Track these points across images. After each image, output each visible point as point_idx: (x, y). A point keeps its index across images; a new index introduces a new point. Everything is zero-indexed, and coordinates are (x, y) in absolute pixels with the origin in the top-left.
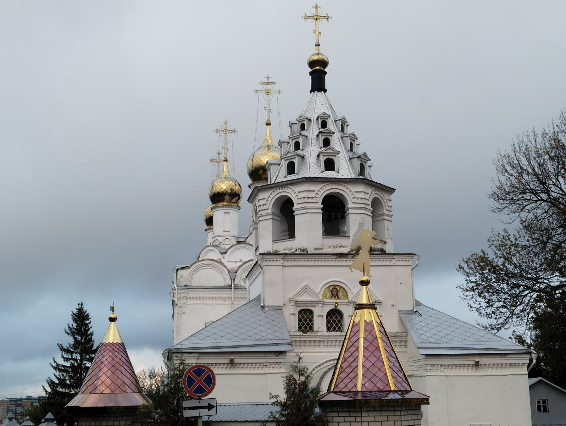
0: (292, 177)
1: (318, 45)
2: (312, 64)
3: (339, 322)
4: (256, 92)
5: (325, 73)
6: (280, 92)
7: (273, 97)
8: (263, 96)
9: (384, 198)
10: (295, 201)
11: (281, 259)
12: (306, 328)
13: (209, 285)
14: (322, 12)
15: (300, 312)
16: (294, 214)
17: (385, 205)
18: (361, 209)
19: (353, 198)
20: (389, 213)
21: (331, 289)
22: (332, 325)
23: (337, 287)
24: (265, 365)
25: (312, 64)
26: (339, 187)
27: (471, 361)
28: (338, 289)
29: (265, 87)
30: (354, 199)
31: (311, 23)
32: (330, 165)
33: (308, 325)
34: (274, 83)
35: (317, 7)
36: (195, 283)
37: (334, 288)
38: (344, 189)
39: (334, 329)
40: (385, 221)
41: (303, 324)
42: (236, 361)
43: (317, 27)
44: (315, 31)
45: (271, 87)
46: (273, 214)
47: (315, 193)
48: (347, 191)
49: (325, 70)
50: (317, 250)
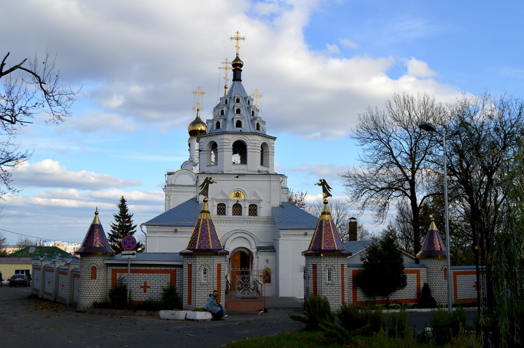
0: (218, 131)
3: (240, 210)
4: (220, 68)
5: (241, 71)
9: (269, 143)
10: (218, 144)
13: (185, 184)
14: (241, 35)
15: (218, 205)
20: (272, 151)
21: (236, 193)
22: (235, 212)
23: (239, 192)
26: (243, 137)
27: (303, 232)
28: (240, 193)
29: (225, 65)
31: (234, 42)
32: (239, 124)
33: (223, 212)
35: (238, 33)
36: (177, 183)
37: (237, 192)
38: (245, 138)
39: (237, 214)
41: (220, 211)
42: (178, 230)
43: (238, 44)
48: (247, 139)
49: (241, 69)
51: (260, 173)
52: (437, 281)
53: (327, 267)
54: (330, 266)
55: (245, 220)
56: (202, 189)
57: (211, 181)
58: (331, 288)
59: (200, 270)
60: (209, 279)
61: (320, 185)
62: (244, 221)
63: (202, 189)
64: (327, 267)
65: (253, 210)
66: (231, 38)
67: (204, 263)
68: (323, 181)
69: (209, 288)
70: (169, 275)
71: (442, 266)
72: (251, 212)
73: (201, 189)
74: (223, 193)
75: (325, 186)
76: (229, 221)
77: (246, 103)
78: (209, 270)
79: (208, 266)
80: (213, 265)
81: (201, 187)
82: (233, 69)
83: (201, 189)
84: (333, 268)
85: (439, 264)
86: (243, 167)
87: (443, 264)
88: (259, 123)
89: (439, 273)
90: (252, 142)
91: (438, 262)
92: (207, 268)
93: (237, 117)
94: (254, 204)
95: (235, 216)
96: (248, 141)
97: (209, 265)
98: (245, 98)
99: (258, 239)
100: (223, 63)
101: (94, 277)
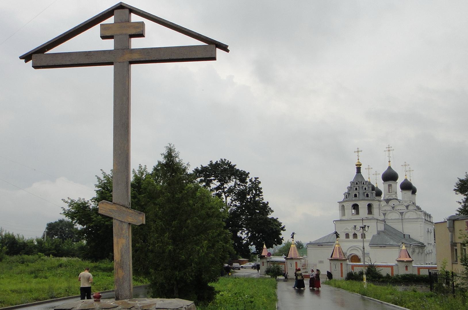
1: (358, 159)
4: (385, 151)
7: (391, 152)
8: (387, 153)
25: (357, 165)
31: (357, 153)
44: (357, 156)
45: (390, 149)
46: (341, 209)
66: (355, 152)
77: (361, 184)
82: (357, 167)
86: (358, 216)
98: (361, 182)
101: (263, 265)
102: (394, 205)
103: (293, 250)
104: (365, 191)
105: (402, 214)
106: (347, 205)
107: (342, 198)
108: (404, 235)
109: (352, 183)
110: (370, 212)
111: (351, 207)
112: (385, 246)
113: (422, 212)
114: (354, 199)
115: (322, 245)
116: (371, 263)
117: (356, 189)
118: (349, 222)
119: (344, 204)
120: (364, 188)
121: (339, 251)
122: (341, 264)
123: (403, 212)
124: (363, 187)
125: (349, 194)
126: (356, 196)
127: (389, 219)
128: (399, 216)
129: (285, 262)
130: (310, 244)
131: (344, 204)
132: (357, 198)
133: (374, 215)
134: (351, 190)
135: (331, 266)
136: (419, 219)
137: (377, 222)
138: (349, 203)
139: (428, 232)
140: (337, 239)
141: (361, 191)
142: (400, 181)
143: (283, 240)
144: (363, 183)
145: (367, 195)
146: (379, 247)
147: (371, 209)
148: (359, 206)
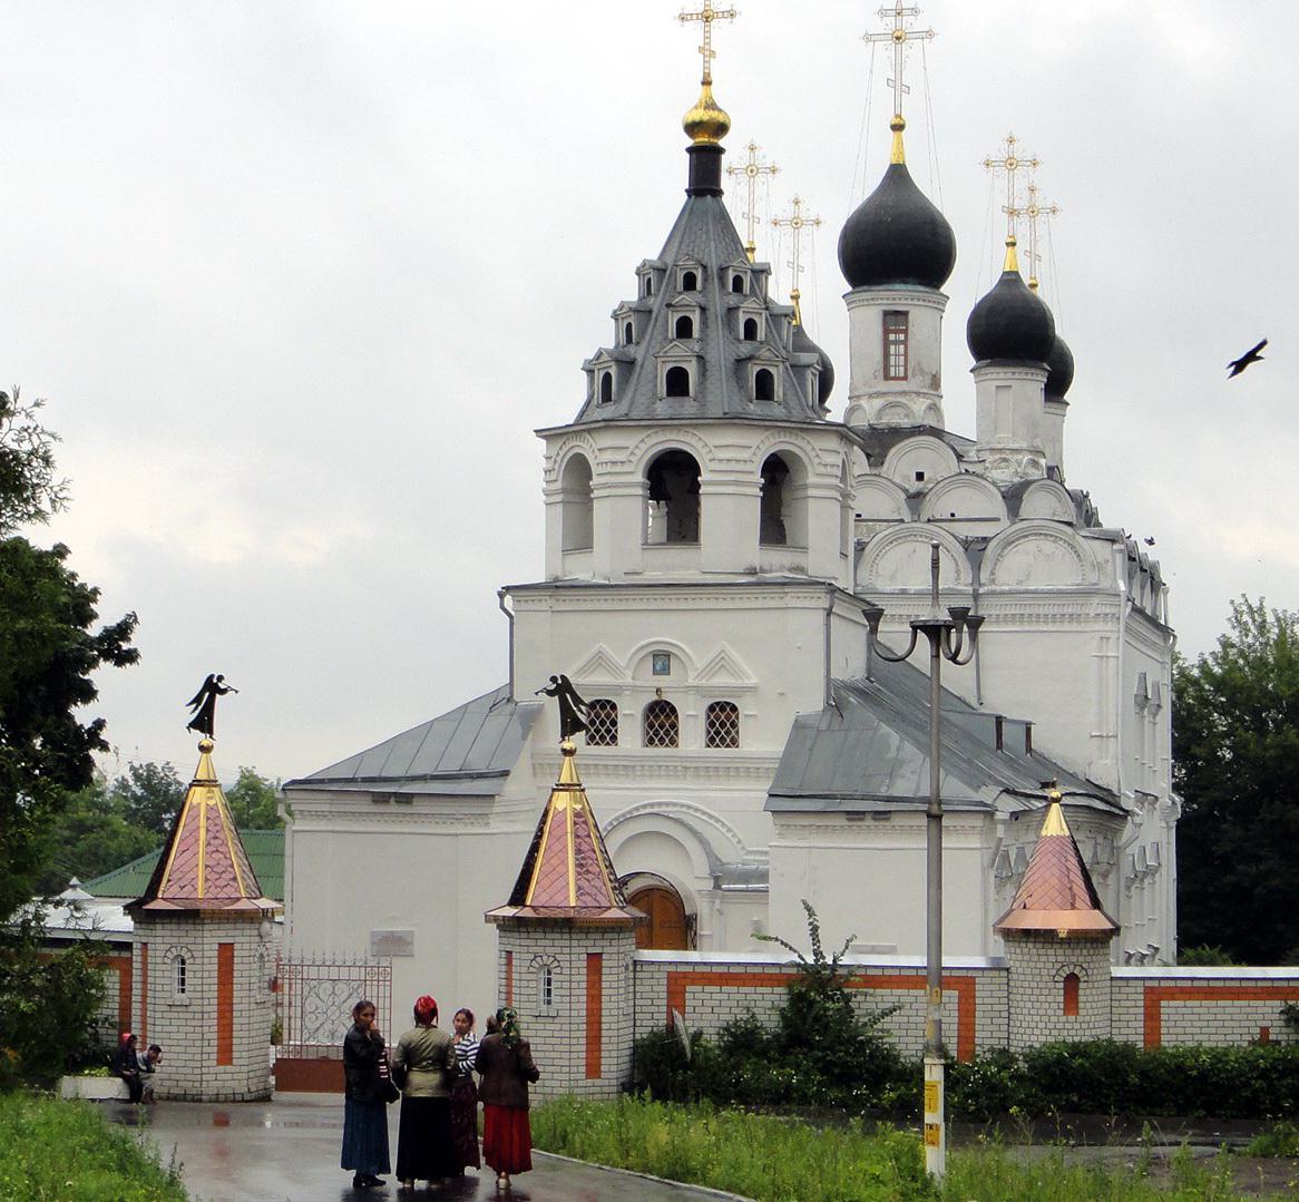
0: (609, 411)
1: (707, 83)
2: (692, 128)
4: (868, 38)
5: (720, 151)
6: (930, 34)
7: (912, 49)
8: (885, 51)
9: (808, 448)
11: (547, 598)
12: (602, 738)
16: (592, 496)
17: (812, 464)
18: (736, 483)
19: (710, 460)
24: (455, 818)
25: (692, 128)
30: (712, 463)
31: (696, 28)
33: (608, 731)
34: (915, 11)
38: (693, 441)
39: (662, 741)
40: (810, 500)
43: (707, 36)
45: (908, 23)
47: (629, 451)
48: (699, 445)
50: (630, 577)
51: (757, 581)
52: (1037, 1018)
53: (538, 959)
54: (545, 958)
55: (688, 765)
56: (200, 708)
57: (221, 686)
58: (548, 1026)
59: (166, 960)
60: (166, 988)
61: (551, 693)
62: (686, 768)
63: (197, 712)
64: (538, 959)
65: (723, 721)
67: (174, 940)
68: (560, 682)
69: (191, 1016)
70: (118, 972)
71: (1058, 966)
72: (717, 733)
73: (193, 711)
74: (599, 661)
75: (568, 695)
76: (627, 768)
77: (723, 285)
78: (191, 961)
79: (189, 950)
80: (201, 947)
81: (194, 706)
82: (690, 142)
83: (193, 711)
84: (556, 964)
85: (1044, 958)
87: (1061, 959)
88: (770, 369)
89: (1046, 992)
90: (720, 454)
91: (1042, 952)
92: (186, 957)
93: (682, 354)
94: (728, 703)
95: (651, 751)
96: (704, 451)
97: (189, 946)
98: (723, 270)
99: (739, 842)
100: (883, 13)
102: (920, 476)
103: (202, 832)
104: (746, 348)
105: (975, 549)
106: (607, 456)
107: (569, 399)
108: (999, 720)
109: (653, 276)
110: (774, 529)
111: (640, 477)
112: (881, 807)
113: (1113, 541)
114: (664, 407)
115: (406, 799)
116: (818, 954)
117: (684, 328)
118: (739, 604)
119: (588, 447)
120: (742, 319)
121: (578, 851)
122: (595, 961)
123: (985, 540)
124: (732, 311)
125: (627, 365)
126: (677, 383)
127: (888, 589)
128: (958, 572)
129: (127, 946)
130: (296, 786)
131: (588, 447)
132: (688, 406)
133: (805, 549)
134: (642, 334)
135: (509, 979)
136: (1096, 600)
137: (829, 612)
138: (629, 440)
139: (1142, 709)
140: (567, 745)
141: (722, 350)
142: (967, 286)
143: (104, 746)
144: (738, 282)
145: (764, 387)
146: (842, 821)
147: (780, 504)
148: (698, 472)
